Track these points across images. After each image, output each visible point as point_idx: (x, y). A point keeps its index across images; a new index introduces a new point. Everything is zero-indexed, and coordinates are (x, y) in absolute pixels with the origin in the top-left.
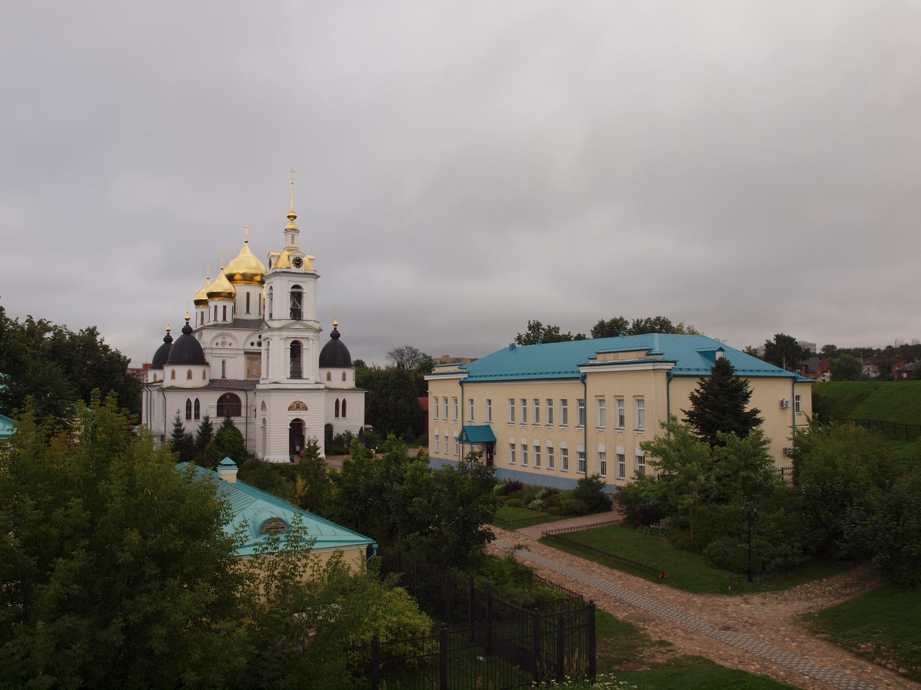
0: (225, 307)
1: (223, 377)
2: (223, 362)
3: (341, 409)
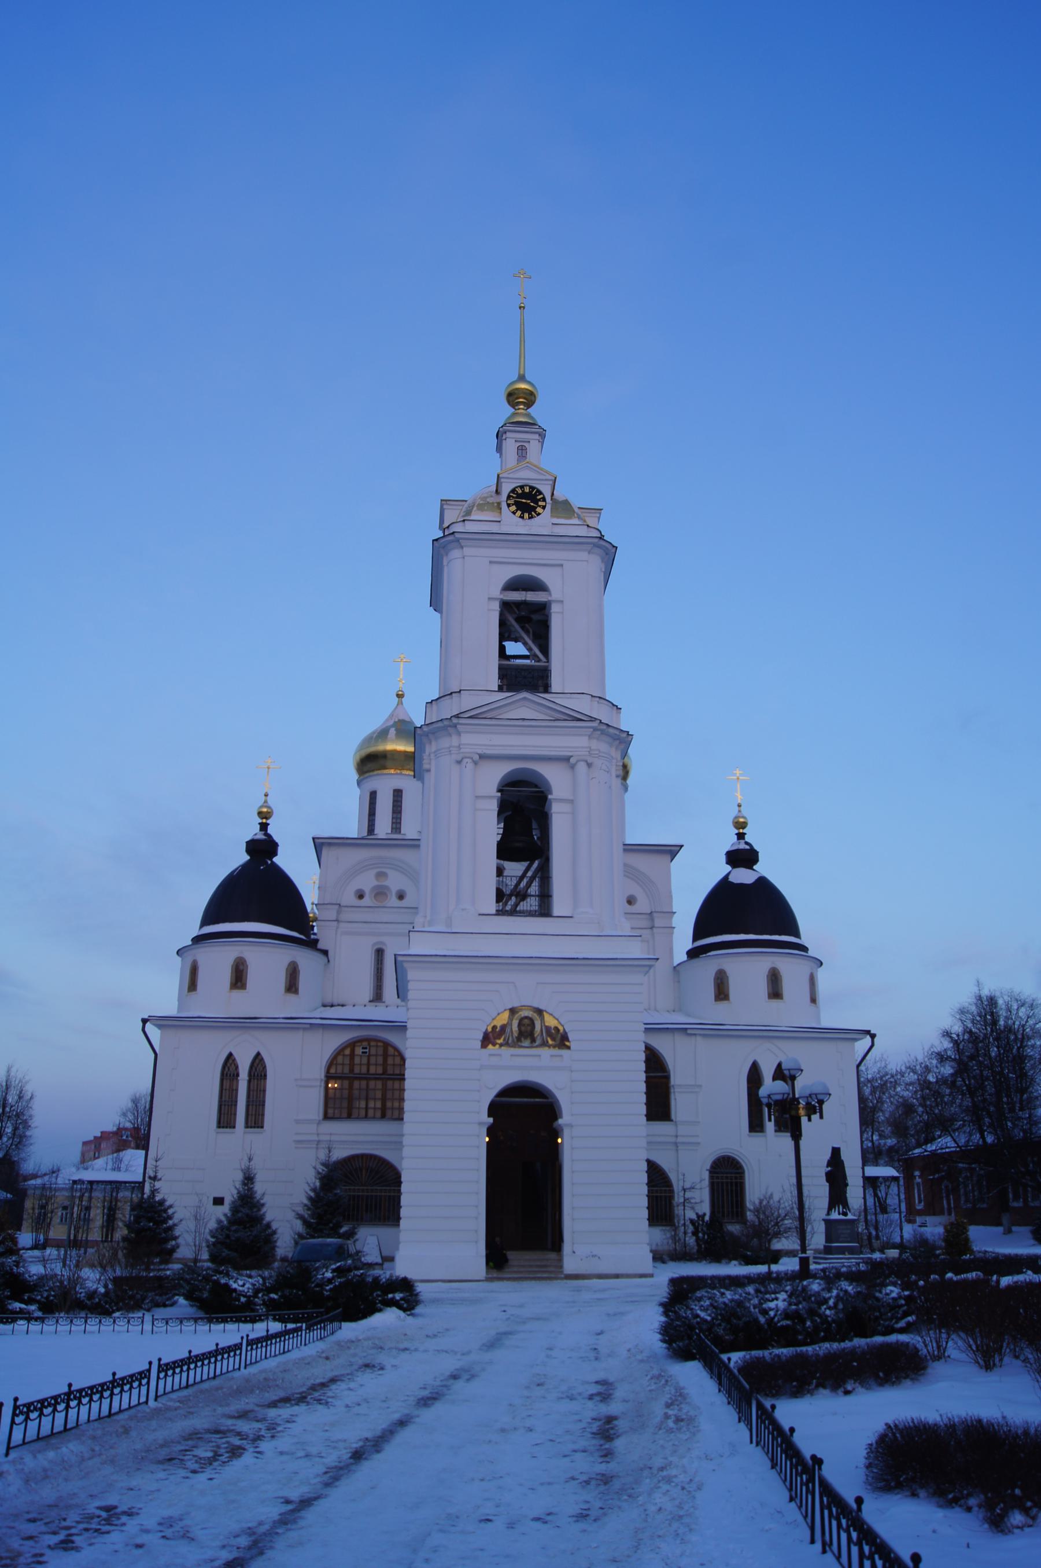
0: (398, 794)
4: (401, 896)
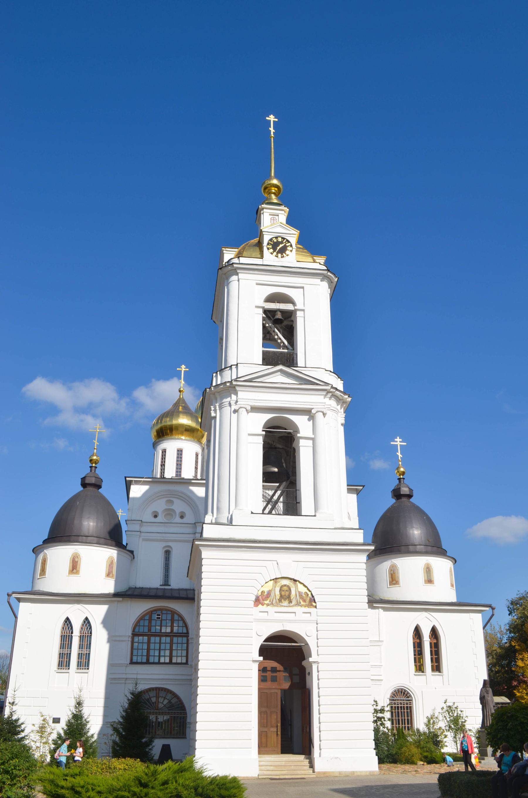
0: (180, 452)
1: (166, 582)
2: (168, 553)
3: (428, 651)
4: (182, 517)
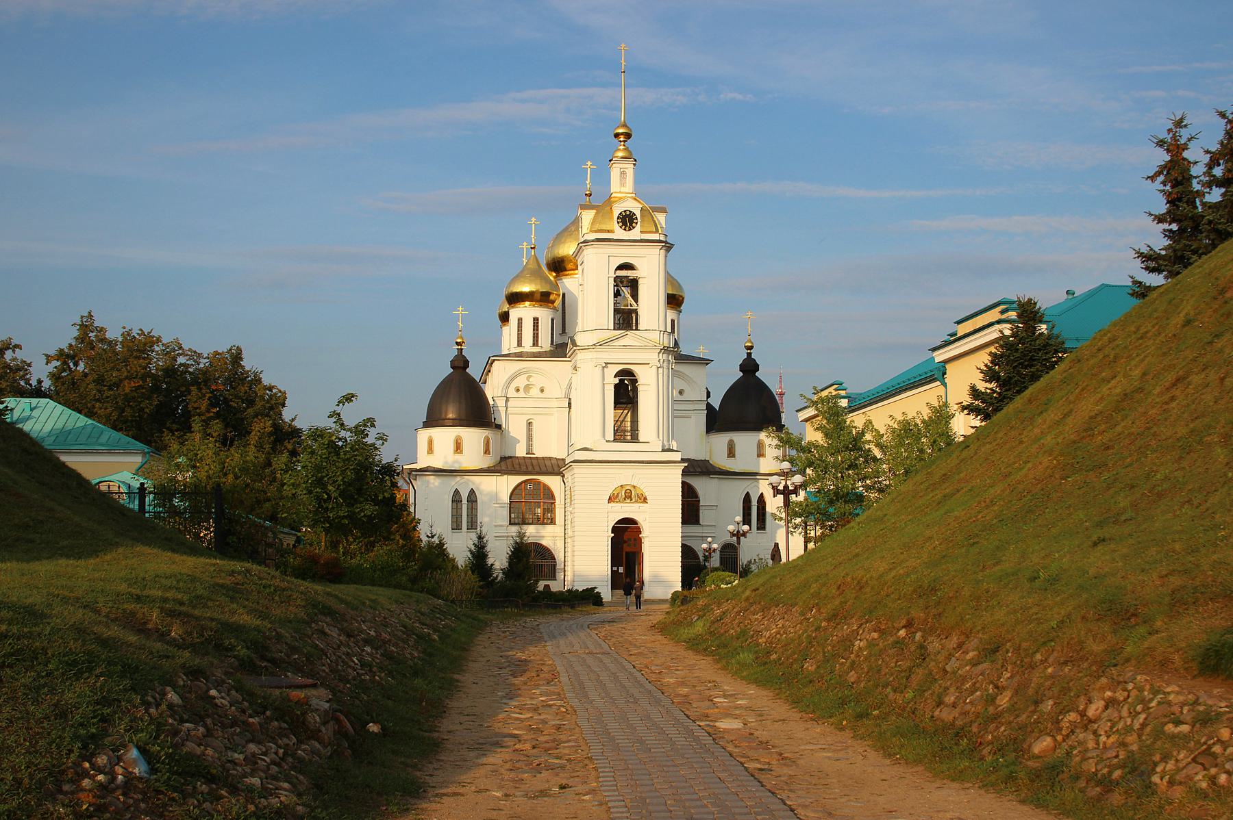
0: (536, 320)
4: (542, 391)
